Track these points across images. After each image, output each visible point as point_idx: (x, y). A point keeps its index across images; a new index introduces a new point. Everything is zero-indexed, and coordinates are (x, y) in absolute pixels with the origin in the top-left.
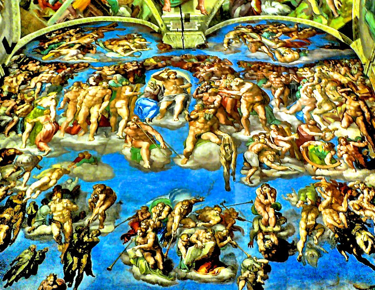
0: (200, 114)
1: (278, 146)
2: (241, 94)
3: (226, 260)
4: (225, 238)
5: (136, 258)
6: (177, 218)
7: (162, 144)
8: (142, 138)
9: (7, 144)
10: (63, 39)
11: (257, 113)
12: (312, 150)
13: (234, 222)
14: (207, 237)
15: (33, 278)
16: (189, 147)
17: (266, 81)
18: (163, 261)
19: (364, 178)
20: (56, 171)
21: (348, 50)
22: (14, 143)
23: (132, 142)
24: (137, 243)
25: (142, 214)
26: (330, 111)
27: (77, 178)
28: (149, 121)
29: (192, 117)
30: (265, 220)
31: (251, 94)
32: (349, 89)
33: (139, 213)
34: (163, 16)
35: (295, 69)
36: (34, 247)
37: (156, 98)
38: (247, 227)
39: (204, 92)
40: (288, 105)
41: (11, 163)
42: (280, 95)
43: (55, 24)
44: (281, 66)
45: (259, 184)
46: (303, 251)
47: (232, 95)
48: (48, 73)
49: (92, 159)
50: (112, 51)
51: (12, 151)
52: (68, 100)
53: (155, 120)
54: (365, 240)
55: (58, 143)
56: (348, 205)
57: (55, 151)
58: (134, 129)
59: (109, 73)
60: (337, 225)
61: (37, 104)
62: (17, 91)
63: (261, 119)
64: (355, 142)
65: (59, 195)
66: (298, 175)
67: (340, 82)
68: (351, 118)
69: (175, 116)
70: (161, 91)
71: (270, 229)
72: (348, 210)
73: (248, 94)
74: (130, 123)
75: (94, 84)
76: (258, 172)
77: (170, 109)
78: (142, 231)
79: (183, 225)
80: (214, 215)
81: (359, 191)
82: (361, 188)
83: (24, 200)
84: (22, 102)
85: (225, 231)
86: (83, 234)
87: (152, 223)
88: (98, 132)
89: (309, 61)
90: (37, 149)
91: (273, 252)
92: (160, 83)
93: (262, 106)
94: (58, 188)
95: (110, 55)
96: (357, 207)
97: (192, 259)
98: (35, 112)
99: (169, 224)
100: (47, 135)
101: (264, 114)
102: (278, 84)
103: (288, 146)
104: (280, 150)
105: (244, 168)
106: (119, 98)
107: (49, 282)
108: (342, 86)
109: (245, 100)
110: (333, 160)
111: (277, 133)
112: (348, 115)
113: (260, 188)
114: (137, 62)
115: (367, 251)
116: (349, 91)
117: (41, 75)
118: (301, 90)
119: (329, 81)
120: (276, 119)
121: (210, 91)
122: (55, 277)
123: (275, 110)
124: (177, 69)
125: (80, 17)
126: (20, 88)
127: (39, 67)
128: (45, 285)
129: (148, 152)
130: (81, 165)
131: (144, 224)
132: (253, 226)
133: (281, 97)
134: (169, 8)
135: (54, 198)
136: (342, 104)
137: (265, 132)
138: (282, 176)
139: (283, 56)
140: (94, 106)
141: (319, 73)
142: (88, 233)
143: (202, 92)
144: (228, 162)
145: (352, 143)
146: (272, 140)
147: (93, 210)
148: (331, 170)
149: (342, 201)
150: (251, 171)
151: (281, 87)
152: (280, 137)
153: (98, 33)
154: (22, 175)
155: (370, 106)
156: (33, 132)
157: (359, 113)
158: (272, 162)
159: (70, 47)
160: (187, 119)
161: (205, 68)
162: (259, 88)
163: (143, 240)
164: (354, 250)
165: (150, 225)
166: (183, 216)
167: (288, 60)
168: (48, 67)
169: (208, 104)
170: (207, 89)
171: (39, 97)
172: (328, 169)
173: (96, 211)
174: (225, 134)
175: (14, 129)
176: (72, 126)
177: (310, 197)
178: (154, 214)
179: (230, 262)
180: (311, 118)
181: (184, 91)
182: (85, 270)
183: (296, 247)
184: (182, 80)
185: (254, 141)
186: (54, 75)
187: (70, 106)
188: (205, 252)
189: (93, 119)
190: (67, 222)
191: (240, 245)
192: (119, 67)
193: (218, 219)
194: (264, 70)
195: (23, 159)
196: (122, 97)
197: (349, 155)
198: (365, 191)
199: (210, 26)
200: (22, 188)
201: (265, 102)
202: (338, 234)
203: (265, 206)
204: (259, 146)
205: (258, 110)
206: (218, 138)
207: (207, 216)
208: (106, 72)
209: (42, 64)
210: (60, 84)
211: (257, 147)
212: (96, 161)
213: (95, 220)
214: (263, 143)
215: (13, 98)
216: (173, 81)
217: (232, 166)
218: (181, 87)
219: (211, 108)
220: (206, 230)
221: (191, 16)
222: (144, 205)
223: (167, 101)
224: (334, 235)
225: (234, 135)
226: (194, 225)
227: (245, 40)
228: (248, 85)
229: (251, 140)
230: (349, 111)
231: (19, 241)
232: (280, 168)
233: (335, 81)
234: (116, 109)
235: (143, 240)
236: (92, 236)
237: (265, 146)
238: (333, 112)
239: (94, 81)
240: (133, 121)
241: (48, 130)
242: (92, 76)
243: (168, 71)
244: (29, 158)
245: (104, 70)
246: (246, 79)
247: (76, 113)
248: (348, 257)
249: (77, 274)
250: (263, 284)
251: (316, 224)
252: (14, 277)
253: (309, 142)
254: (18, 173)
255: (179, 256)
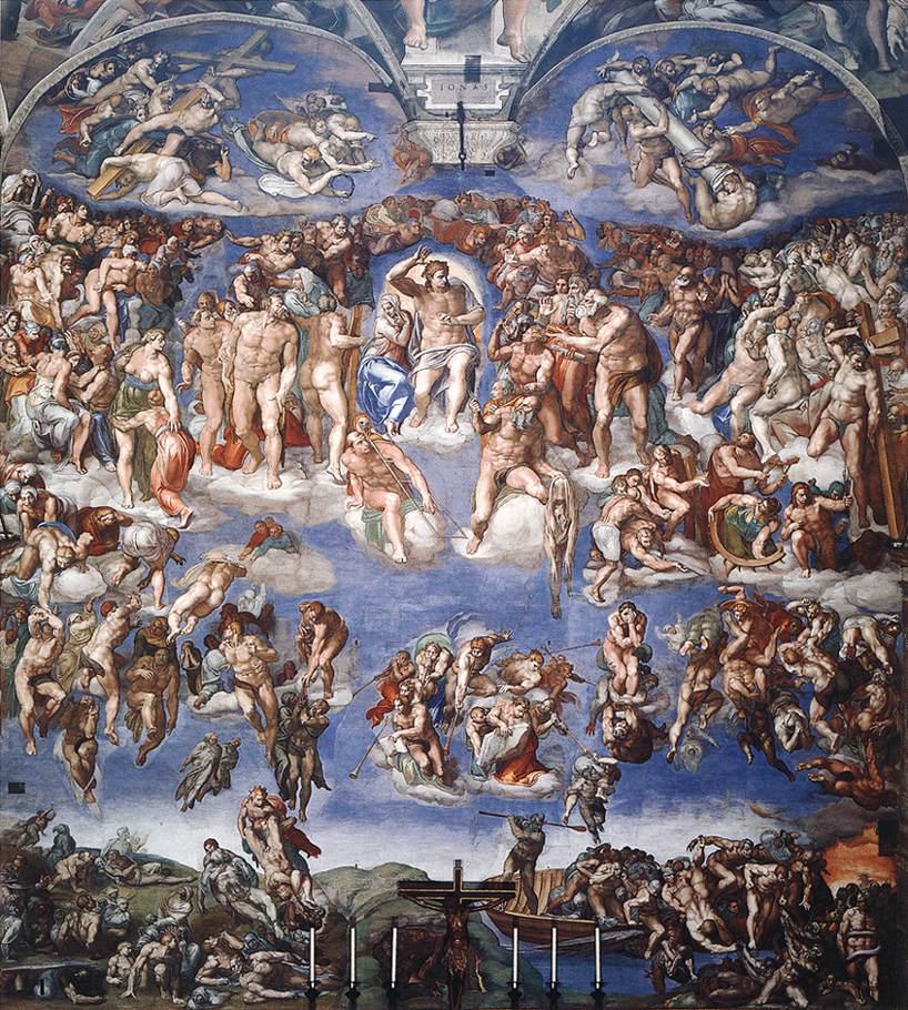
0: (505, 410)
1: (663, 508)
2: (597, 348)
3: (547, 757)
4: (546, 716)
5: (397, 754)
6: (463, 677)
7: (426, 497)
8: (382, 481)
9: (88, 497)
10: (125, 109)
11: (628, 412)
12: (731, 519)
13: (564, 683)
14: (517, 712)
15: (225, 794)
16: (482, 511)
17: (662, 302)
18: (442, 760)
19: (820, 592)
20: (217, 568)
21: (889, 172)
22: (103, 489)
23: (362, 495)
24: (395, 726)
25: (400, 666)
26: (792, 404)
27: (263, 585)
28: (394, 430)
29: (488, 420)
30: (619, 679)
31: (621, 348)
32: (853, 331)
33: (395, 665)
34: (406, 62)
35: (737, 252)
36: (214, 737)
37: (404, 362)
38: (586, 695)
39: (514, 340)
40: (700, 385)
41: (115, 549)
42: (687, 351)
43: (90, 45)
44: (704, 243)
45: (616, 602)
46: (678, 744)
47: (578, 350)
48: (122, 257)
49: (285, 538)
50: (273, 169)
51: (108, 518)
52: (197, 361)
53: (408, 431)
54: (790, 723)
55: (201, 494)
56: (776, 651)
57: (204, 515)
58: (364, 455)
59: (281, 262)
60: (745, 692)
61: (123, 369)
62: (59, 320)
63: (637, 428)
64: (827, 497)
65: (235, 625)
66: (693, 580)
67: (839, 304)
68: (834, 428)
69: (450, 419)
70: (413, 325)
71: (626, 698)
72: (774, 661)
73: (614, 348)
74: (352, 437)
75: (247, 300)
76: (616, 575)
77: (436, 391)
78: (402, 703)
79: (474, 689)
80: (529, 670)
81: (803, 620)
82: (809, 615)
83: (169, 638)
84: (85, 363)
85: (547, 703)
86: (297, 709)
87: (418, 685)
88: (287, 464)
89: (780, 221)
90: (160, 511)
91: (627, 744)
92: (408, 304)
93: (642, 389)
94: (230, 611)
95: (272, 185)
96: (790, 657)
97: (491, 757)
98: (126, 394)
99: (449, 689)
100: (172, 470)
101: (644, 413)
102: (689, 313)
103: (681, 506)
104: (665, 517)
105: (591, 564)
106: (317, 356)
107: (255, 800)
108: (840, 317)
109: (607, 368)
110: (769, 549)
111: (665, 470)
112: (830, 416)
113: (617, 613)
114: (347, 222)
115: (788, 746)
116: (852, 337)
117: (105, 263)
118: (740, 334)
119: (810, 300)
120: (669, 430)
121: (527, 337)
122: (263, 791)
123: (671, 400)
124: (448, 256)
125: (157, 18)
126: (65, 313)
127: (89, 227)
128: (250, 806)
129: (399, 520)
130: (263, 553)
131: (404, 688)
132: (597, 693)
133: (688, 358)
134: (424, 38)
135: (228, 633)
136: (826, 379)
137: (639, 466)
138: (662, 584)
139: (716, 201)
140: (263, 382)
141: (795, 271)
142: (306, 706)
143: (511, 340)
144: (560, 549)
145: (819, 500)
146: (653, 491)
147: (307, 659)
148: (763, 571)
149: (767, 645)
150: (606, 570)
151: (694, 323)
152: (672, 483)
153: (222, 83)
154: (149, 579)
155: (886, 388)
156: (140, 458)
157: (856, 411)
158: (647, 550)
159: (154, 142)
160: (477, 427)
161: (518, 247)
162: (641, 325)
163: (405, 721)
164: (766, 745)
165: (415, 689)
166: (474, 672)
167: (726, 218)
168: (114, 232)
169: (523, 378)
170: (522, 328)
171: (123, 346)
172: (753, 569)
173: (313, 662)
174: (556, 473)
175: (90, 449)
176: (223, 442)
177: (707, 634)
178: (421, 667)
179: (553, 761)
180: (747, 428)
181: (466, 334)
182: (313, 777)
183: (668, 734)
184: (461, 291)
185: (614, 492)
186: (140, 265)
187: (206, 376)
188: (514, 741)
189: (269, 424)
190: (264, 685)
191: (573, 730)
192: (302, 241)
193: (536, 677)
194: (663, 261)
195: (137, 536)
196: (326, 354)
197: (806, 532)
198: (816, 623)
199: (533, 82)
200: (155, 610)
201: (649, 377)
202: (746, 712)
203: (622, 652)
204: (626, 504)
205: (632, 399)
206: (542, 483)
207: (517, 671)
208: (272, 256)
209: (96, 216)
210: (164, 301)
211: (619, 509)
212: (291, 544)
213: (315, 679)
214: (634, 499)
215: (58, 348)
216: (439, 297)
217: (567, 559)
218: (459, 318)
219: (530, 394)
220: (514, 699)
221: (483, 62)
222: (402, 649)
223: (431, 367)
224: (737, 714)
225: (576, 474)
226: (494, 690)
227: (626, 131)
228: (618, 317)
229: (610, 490)
230: (837, 403)
231: (184, 724)
232: (662, 565)
233: (827, 299)
234: (316, 390)
235: (405, 721)
236: (314, 713)
237: (637, 506)
238: (798, 408)
239: (247, 294)
240: (359, 430)
241: (173, 454)
242: (240, 273)
243: (427, 260)
244: (151, 535)
245: (266, 251)
246: (615, 296)
247: (226, 406)
248: (752, 756)
249: (300, 787)
250: (606, 802)
251: (710, 690)
252: (192, 795)
253: (729, 497)
254: (137, 572)
255: (469, 751)
